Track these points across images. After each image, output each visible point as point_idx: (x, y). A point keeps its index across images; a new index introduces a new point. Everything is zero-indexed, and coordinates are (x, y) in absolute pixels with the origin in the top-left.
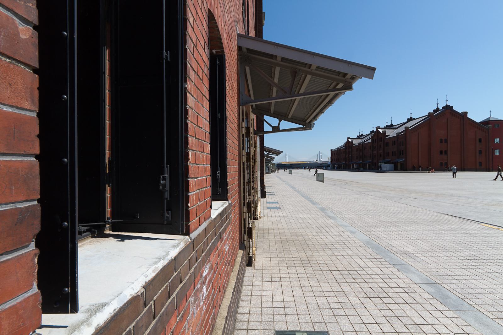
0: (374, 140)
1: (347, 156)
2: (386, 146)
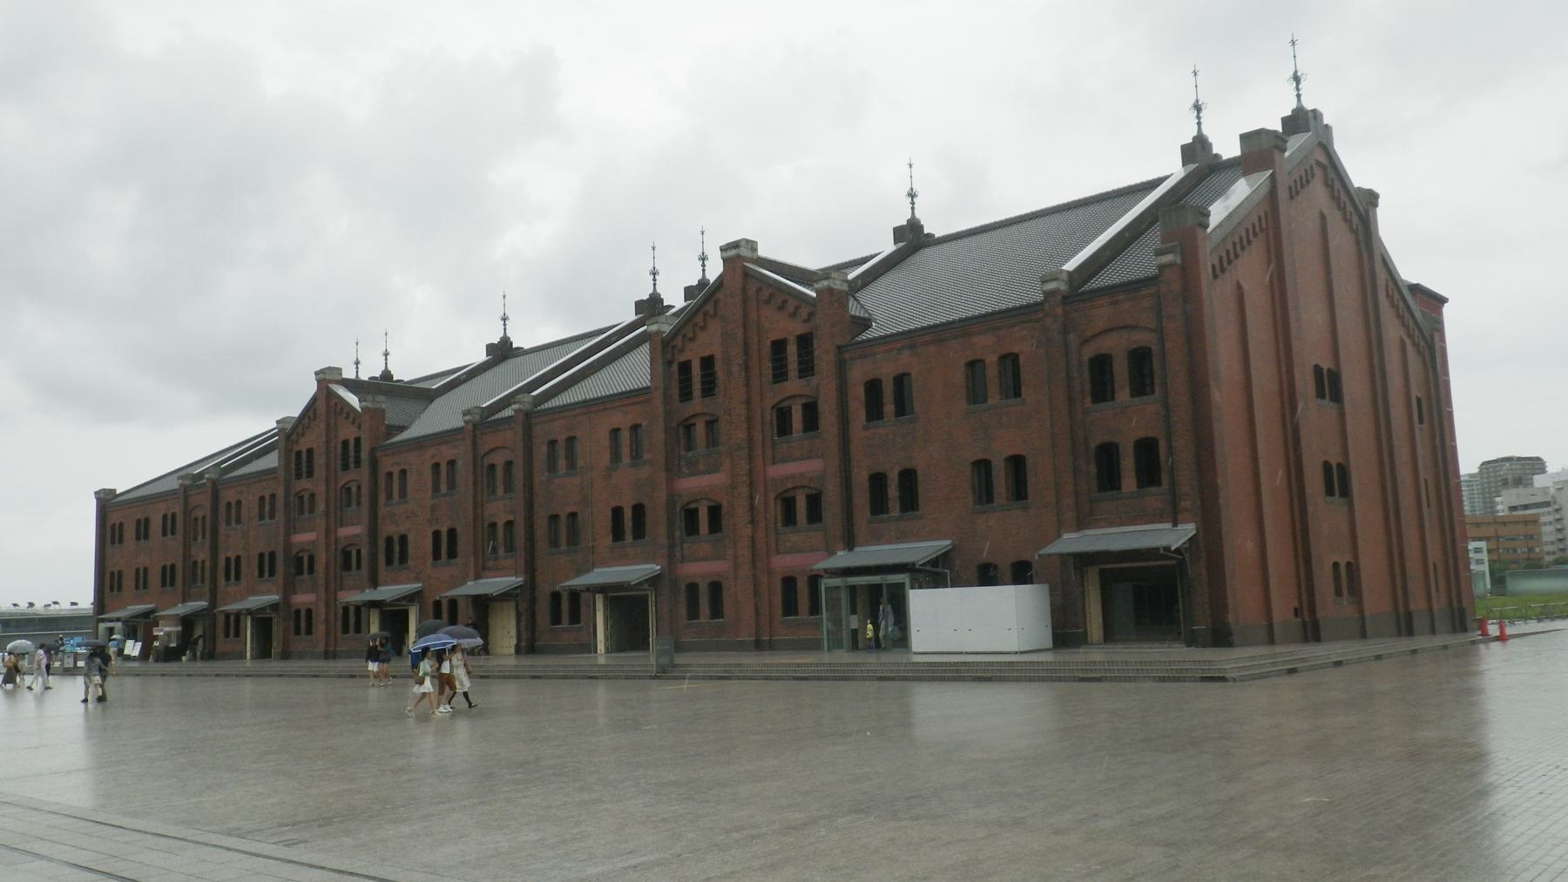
0: (685, 367)
2: (874, 411)
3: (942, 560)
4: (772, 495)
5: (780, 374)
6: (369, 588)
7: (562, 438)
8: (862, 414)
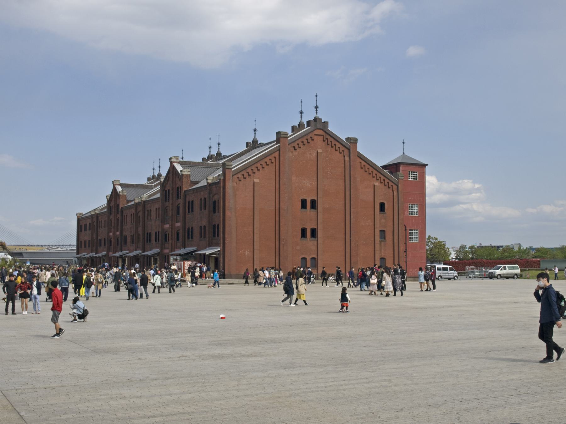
0: (166, 191)
4: (176, 231)
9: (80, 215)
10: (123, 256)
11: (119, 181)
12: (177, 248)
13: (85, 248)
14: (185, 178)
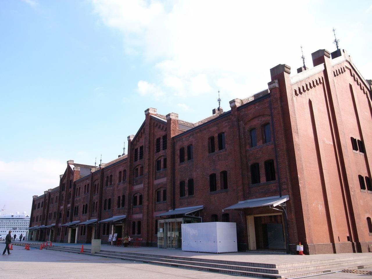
0: (136, 150)
1: (62, 207)
2: (182, 160)
3: (197, 213)
4: (154, 191)
5: (158, 150)
6: (70, 222)
7: (109, 176)
8: (179, 160)
9: (35, 197)
10: (76, 225)
11: (73, 161)
12: (155, 211)
13: (36, 222)
14: (173, 123)
